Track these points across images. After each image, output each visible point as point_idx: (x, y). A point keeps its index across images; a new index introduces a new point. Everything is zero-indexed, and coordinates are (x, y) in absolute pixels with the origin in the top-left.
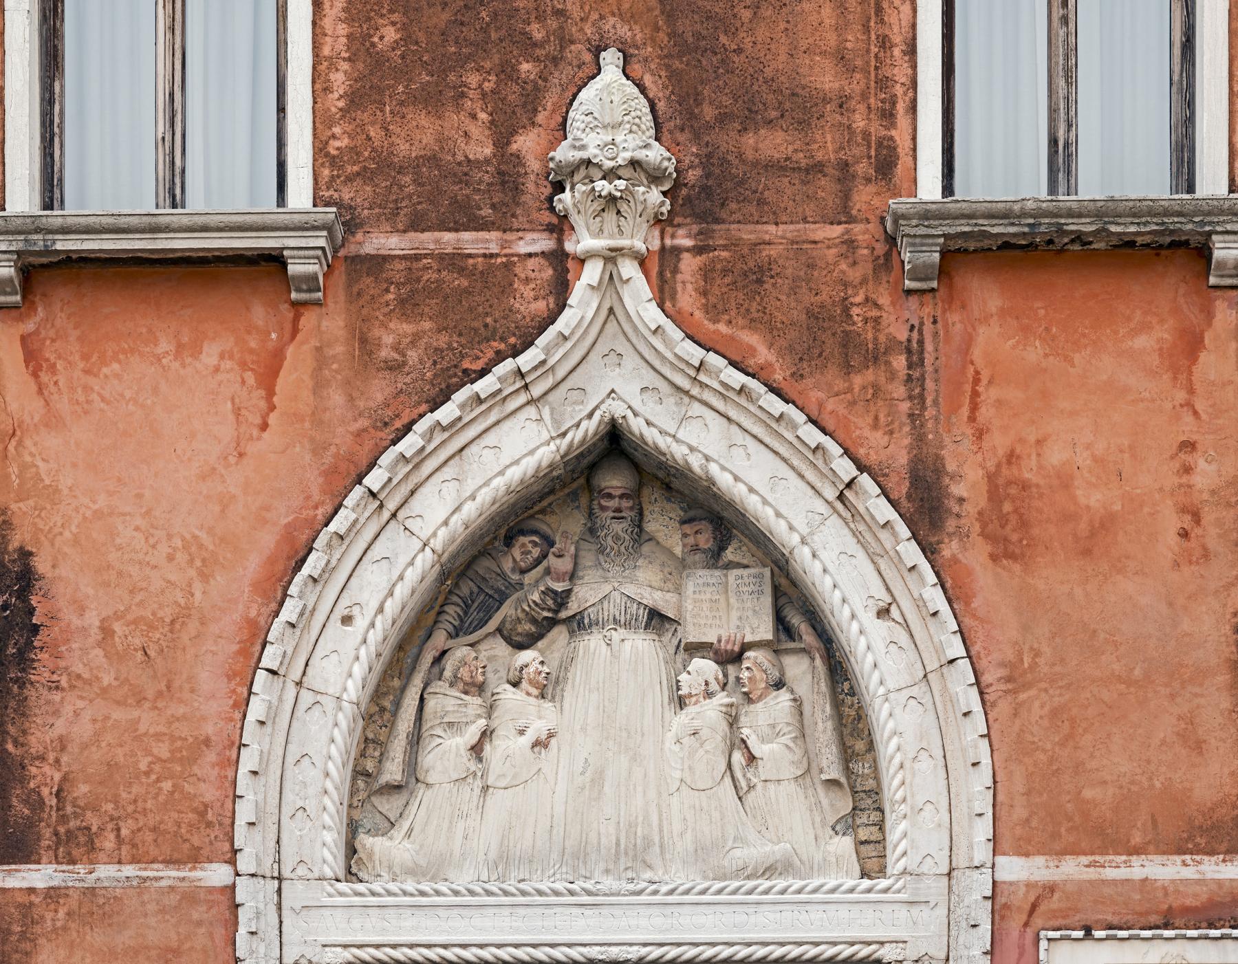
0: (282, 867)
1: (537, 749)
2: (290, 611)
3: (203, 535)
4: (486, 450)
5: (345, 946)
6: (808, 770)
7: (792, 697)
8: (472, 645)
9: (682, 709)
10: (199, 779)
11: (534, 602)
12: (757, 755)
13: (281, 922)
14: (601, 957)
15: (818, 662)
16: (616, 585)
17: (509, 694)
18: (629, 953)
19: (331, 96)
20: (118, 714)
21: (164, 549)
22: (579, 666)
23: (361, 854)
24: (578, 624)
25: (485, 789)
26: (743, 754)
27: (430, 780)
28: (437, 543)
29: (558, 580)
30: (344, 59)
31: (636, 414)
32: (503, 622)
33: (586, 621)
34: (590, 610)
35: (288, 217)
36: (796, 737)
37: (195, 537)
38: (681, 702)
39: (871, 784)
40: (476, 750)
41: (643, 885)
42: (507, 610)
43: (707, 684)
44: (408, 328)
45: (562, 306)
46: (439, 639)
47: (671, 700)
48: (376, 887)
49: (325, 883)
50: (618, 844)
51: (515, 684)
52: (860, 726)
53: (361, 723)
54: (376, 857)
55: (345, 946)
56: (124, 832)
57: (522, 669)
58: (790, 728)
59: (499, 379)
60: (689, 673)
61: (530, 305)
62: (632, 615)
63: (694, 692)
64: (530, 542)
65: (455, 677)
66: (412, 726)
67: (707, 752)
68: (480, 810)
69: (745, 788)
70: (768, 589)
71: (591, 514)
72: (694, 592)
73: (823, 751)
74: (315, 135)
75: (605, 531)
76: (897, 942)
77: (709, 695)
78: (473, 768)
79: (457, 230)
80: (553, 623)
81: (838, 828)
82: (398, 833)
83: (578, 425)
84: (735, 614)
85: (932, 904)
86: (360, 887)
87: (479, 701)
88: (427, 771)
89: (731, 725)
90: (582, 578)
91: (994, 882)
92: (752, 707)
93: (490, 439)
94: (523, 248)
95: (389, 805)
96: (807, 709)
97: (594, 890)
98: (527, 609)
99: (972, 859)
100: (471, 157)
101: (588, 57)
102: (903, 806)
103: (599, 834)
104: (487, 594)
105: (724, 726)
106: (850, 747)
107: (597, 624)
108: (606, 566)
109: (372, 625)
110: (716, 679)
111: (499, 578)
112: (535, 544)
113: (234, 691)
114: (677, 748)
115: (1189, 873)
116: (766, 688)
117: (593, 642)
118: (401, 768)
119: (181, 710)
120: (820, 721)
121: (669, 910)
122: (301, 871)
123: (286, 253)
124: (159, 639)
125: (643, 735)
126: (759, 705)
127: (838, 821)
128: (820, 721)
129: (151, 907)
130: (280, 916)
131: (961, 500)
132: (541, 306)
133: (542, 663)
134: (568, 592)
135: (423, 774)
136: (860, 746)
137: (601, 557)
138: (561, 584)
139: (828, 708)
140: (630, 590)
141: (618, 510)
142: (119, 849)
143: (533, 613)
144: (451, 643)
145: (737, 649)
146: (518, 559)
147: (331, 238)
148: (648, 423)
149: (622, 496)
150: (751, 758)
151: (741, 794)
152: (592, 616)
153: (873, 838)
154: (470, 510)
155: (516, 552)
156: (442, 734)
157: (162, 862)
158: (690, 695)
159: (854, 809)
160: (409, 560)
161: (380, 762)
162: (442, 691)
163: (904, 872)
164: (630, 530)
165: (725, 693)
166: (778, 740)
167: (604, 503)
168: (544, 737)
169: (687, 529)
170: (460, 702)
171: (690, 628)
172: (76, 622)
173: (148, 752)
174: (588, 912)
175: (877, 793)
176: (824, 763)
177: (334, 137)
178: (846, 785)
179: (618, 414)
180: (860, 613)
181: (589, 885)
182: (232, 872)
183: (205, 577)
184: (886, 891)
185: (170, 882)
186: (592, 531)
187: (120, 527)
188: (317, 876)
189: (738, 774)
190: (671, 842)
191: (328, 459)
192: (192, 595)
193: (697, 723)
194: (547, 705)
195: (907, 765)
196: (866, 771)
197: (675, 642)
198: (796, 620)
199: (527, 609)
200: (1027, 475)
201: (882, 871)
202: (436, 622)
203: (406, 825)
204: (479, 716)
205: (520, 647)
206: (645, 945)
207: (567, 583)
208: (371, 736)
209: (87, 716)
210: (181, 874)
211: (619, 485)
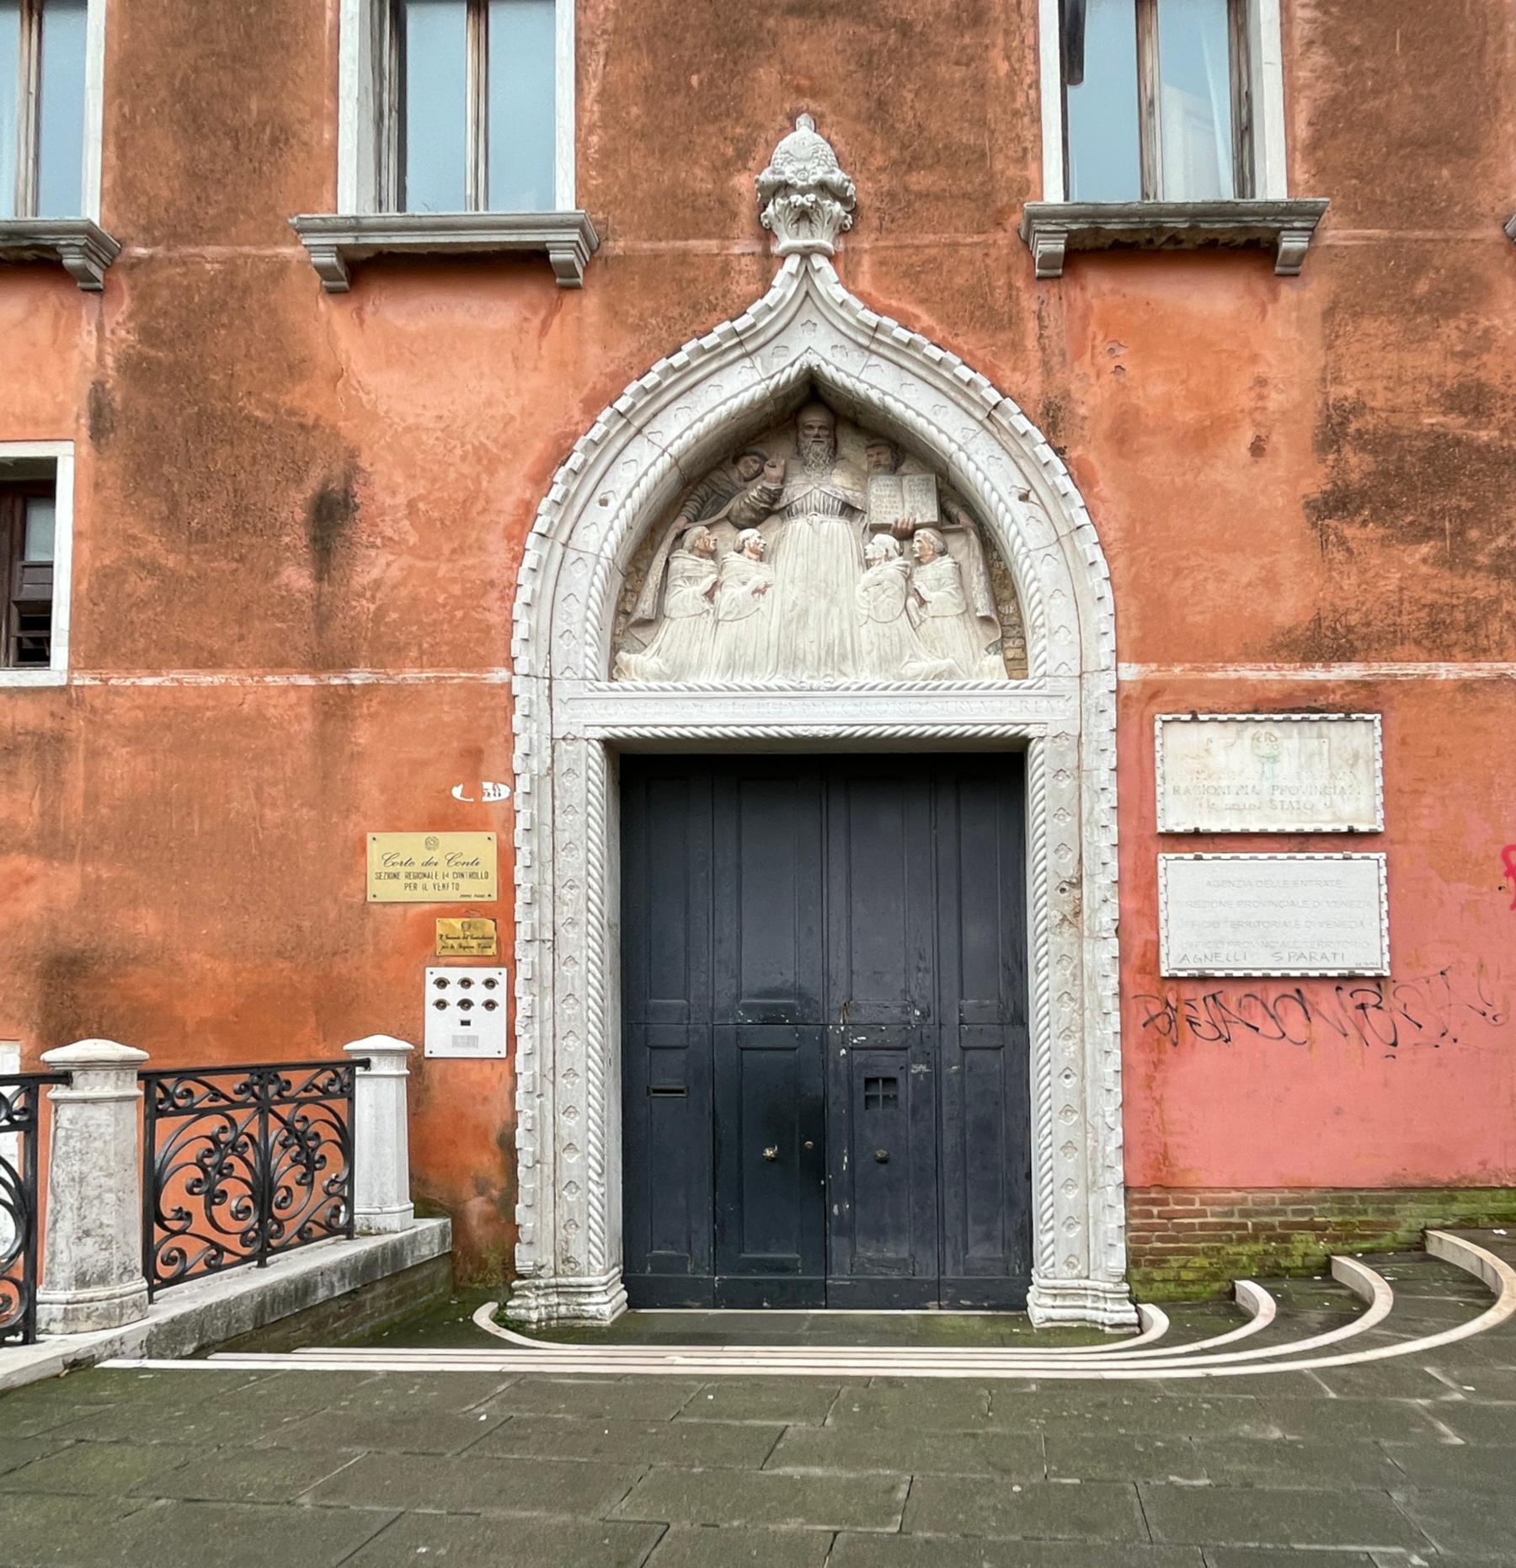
2: (556, 493)
3: (489, 444)
5: (603, 726)
6: (967, 611)
15: (973, 536)
20: (420, 564)
21: (458, 452)
24: (786, 513)
28: (673, 450)
29: (770, 481)
31: (828, 363)
37: (482, 444)
44: (648, 304)
45: (767, 286)
47: (860, 563)
55: (603, 726)
56: (425, 645)
77: (888, 558)
79: (686, 239)
83: (782, 371)
84: (908, 506)
91: (1118, 681)
94: (737, 250)
96: (965, 569)
109: (623, 505)
115: (1272, 675)
117: (798, 525)
119: (471, 562)
121: (858, 701)
122: (568, 674)
129: (447, 698)
131: (1084, 418)
132: (753, 288)
139: (981, 567)
148: (838, 369)
150: (923, 603)
163: (1044, 675)
169: (871, 452)
171: (873, 514)
172: (389, 501)
173: (445, 591)
174: (793, 702)
179: (814, 363)
180: (1005, 496)
183: (492, 473)
184: (1030, 688)
187: (424, 438)
191: (586, 391)
195: (1045, 601)
198: (955, 510)
200: (1135, 401)
209: (395, 566)
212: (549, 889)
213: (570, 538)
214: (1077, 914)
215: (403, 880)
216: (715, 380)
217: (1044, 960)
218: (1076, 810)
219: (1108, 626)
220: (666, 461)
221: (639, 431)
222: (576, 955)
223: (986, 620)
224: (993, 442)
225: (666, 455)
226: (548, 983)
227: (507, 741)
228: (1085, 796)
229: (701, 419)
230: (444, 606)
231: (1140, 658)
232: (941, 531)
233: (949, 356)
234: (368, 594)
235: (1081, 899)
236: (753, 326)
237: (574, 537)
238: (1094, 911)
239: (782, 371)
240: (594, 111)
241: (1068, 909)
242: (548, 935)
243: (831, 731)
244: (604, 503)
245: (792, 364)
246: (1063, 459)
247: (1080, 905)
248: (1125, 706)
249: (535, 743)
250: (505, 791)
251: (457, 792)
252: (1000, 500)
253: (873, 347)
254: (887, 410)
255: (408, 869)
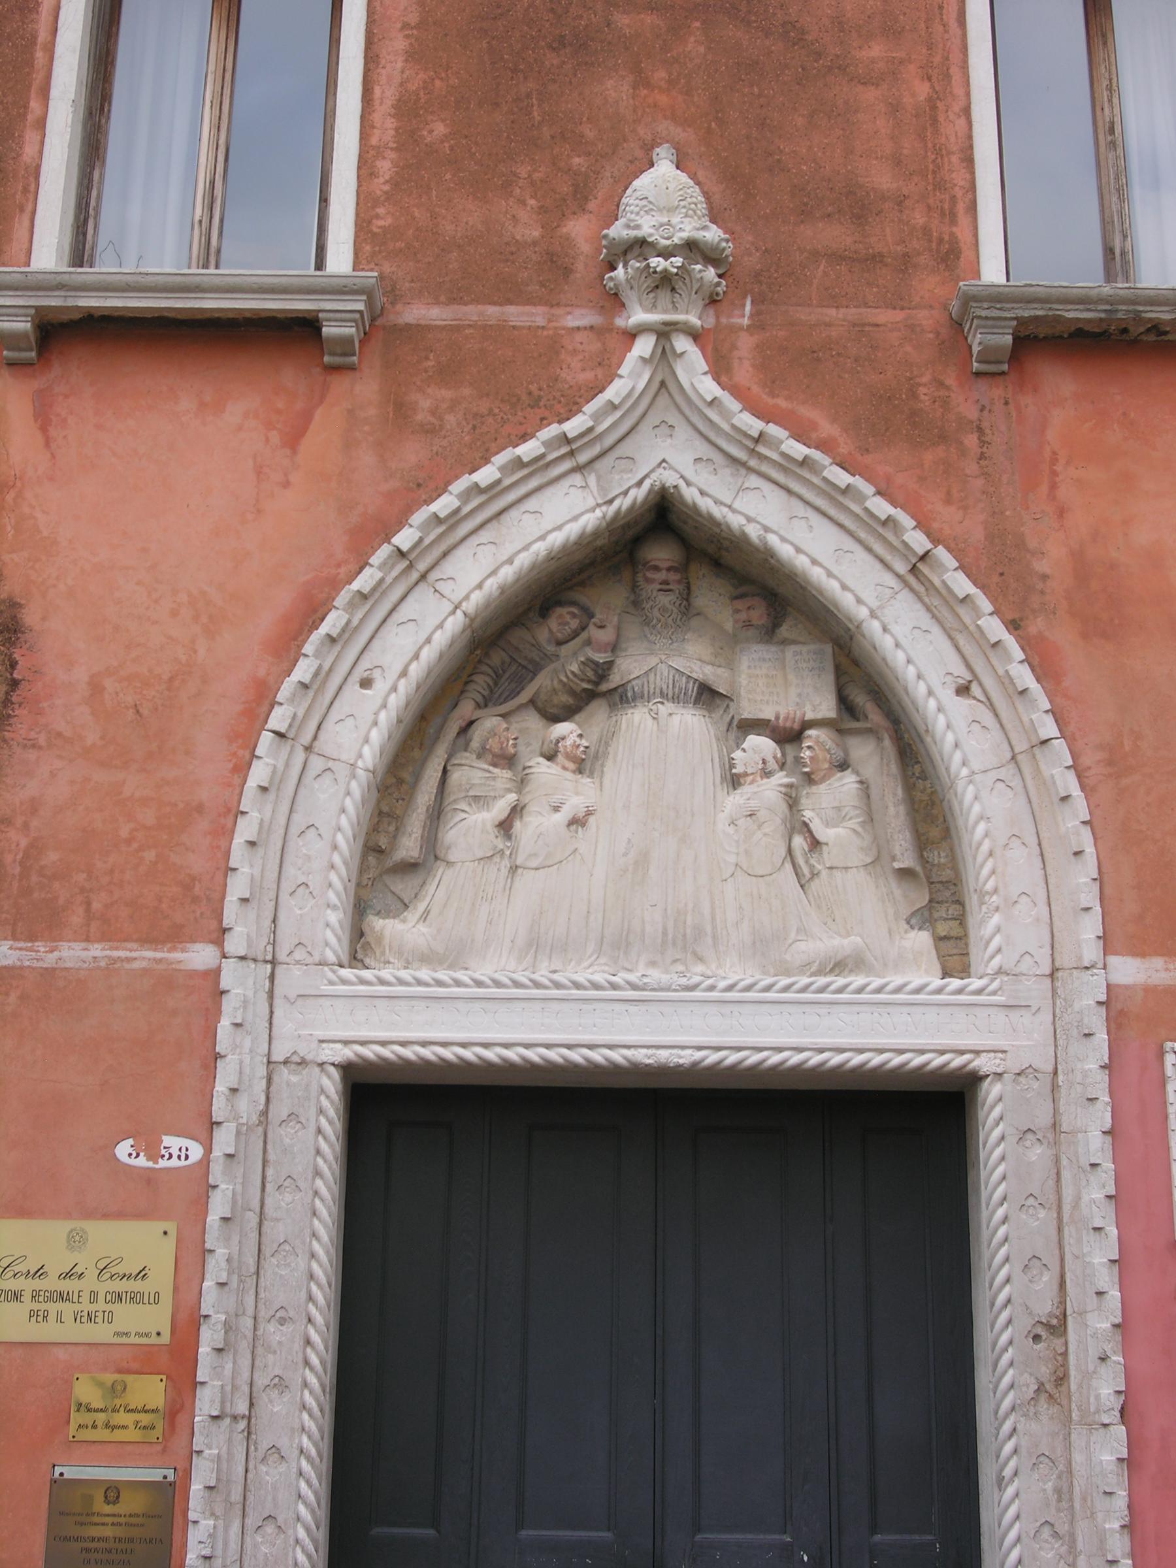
0: (277, 949)
1: (573, 828)
2: (303, 671)
4: (527, 515)
5: (346, 1043)
7: (858, 779)
8: (503, 716)
9: (735, 789)
10: (187, 849)
11: (573, 672)
12: (821, 838)
13: (272, 1013)
14: (648, 1061)
15: (887, 742)
16: (663, 657)
17: (542, 769)
18: (681, 1057)
19: (376, 180)
22: (621, 741)
23: (369, 938)
24: (620, 698)
25: (514, 869)
26: (805, 838)
27: (451, 858)
28: (470, 606)
29: (600, 651)
30: (392, 149)
32: (537, 693)
33: (630, 694)
34: (634, 683)
35: (324, 280)
36: (864, 822)
38: (734, 781)
39: (947, 874)
40: (505, 826)
41: (696, 979)
42: (543, 682)
43: (764, 762)
44: (447, 394)
46: (466, 709)
47: (723, 779)
48: (386, 974)
49: (326, 968)
50: (665, 933)
51: (550, 757)
52: (935, 812)
53: (375, 794)
54: (386, 942)
55: (346, 1043)
56: (96, 906)
57: (558, 742)
58: (858, 812)
59: (543, 443)
60: (744, 750)
61: (575, 373)
62: (681, 689)
63: (749, 771)
64: (568, 613)
65: (484, 748)
66: (433, 799)
67: (765, 835)
68: (508, 892)
69: (808, 875)
70: (830, 668)
71: (634, 588)
72: (749, 667)
73: (896, 837)
74: (357, 215)
75: (651, 603)
76: (995, 1051)
77: (767, 774)
78: (501, 846)
79: (501, 305)
80: (591, 696)
81: (913, 921)
82: (412, 916)
83: (625, 493)
85: (1034, 1009)
86: (366, 974)
87: (507, 774)
88: (449, 848)
89: (791, 807)
90: (626, 650)
91: (1108, 986)
92: (814, 789)
93: (531, 505)
95: (402, 886)
96: (875, 792)
97: (641, 983)
98: (565, 679)
99: (1080, 958)
100: (518, 237)
101: (639, 153)
102: (994, 898)
103: (643, 922)
104: (520, 664)
105: (784, 807)
106: (923, 834)
107: (642, 697)
108: (653, 638)
109: (394, 689)
110: (775, 757)
111: (533, 649)
112: (574, 616)
113: (234, 754)
114: (731, 830)
116: (830, 769)
117: (637, 717)
118: (418, 844)
120: (890, 805)
121: (727, 1009)
122: (299, 954)
123: (321, 315)
124: (154, 697)
125: (693, 815)
126: (822, 787)
127: (913, 914)
128: (890, 805)
130: (271, 1006)
133: (580, 736)
134: (610, 664)
135: (443, 852)
136: (935, 833)
137: (646, 629)
138: (603, 655)
139: (900, 792)
140: (677, 663)
141: (666, 583)
142: (88, 925)
143: (571, 684)
144: (478, 713)
145: (796, 726)
146: (554, 630)
147: (370, 303)
149: (669, 569)
150: (815, 844)
151: (803, 882)
152: (636, 689)
153: (953, 933)
154: (507, 573)
155: (553, 623)
156: (467, 808)
157: (136, 941)
158: (746, 774)
159: (930, 901)
160: (437, 622)
161: (395, 837)
162: (467, 762)
163: (1000, 971)
164: (678, 602)
165: (784, 773)
166: (844, 824)
167: (649, 575)
168: (581, 815)
169: (739, 604)
170: (488, 775)
171: (744, 703)
174: (633, 1009)
175: (955, 884)
176: (897, 851)
177: (377, 217)
178: (922, 875)
181: (633, 977)
182: (218, 954)
184: (979, 992)
185: (144, 964)
186: (636, 604)
188: (317, 959)
189: (801, 861)
190: (724, 933)
192: (195, 652)
193: (753, 804)
194: (586, 780)
196: (942, 860)
197: (727, 719)
198: (860, 699)
199: (565, 679)
201: (964, 971)
202: (462, 692)
203: (422, 907)
204: (509, 791)
205: (556, 719)
206: (700, 1048)
207: (609, 654)
208: (385, 809)
210: (159, 955)
211: (667, 557)
212: (249, 1322)
213: (315, 738)
214: (1061, 1379)
215: (28, 1304)
216: (531, 504)
217: (1012, 1464)
218: (1052, 1198)
219: (1090, 896)
220: (455, 623)
221: (423, 577)
222: (284, 1443)
223: (905, 874)
224: (919, 606)
225: (459, 613)
226: (236, 1496)
227: (205, 1066)
228: (1066, 1175)
229: (510, 561)
230: (128, 842)
231: (1139, 949)
232: (840, 731)
233: (858, 482)
234: (19, 821)
235: (1065, 1354)
236: (590, 430)
237: (322, 736)
238: (1087, 1376)
239: (625, 493)
240: (386, 128)
241: (1045, 1371)
242: (242, 1408)
243: (685, 1058)
244: (366, 683)
245: (639, 484)
246: (1019, 639)
247: (1065, 1365)
248: (1119, 1026)
249: (247, 1070)
250: (196, 1152)
251: (123, 1150)
252: (930, 693)
253: (753, 463)
254: (768, 554)
255: (37, 1284)
